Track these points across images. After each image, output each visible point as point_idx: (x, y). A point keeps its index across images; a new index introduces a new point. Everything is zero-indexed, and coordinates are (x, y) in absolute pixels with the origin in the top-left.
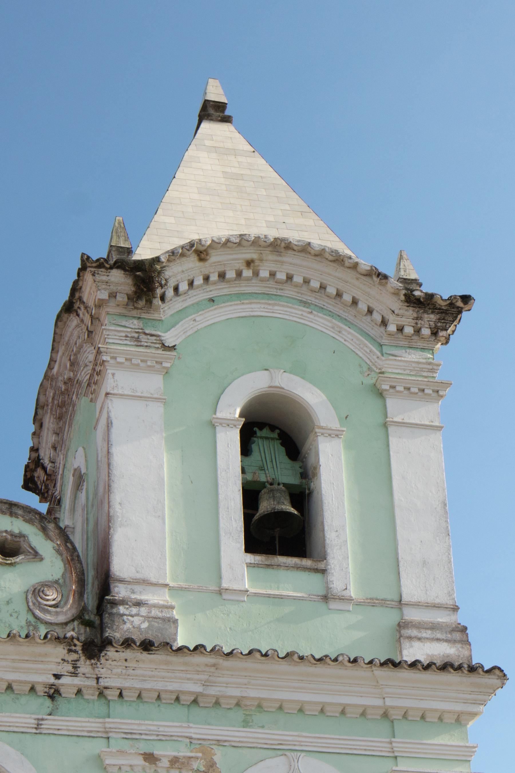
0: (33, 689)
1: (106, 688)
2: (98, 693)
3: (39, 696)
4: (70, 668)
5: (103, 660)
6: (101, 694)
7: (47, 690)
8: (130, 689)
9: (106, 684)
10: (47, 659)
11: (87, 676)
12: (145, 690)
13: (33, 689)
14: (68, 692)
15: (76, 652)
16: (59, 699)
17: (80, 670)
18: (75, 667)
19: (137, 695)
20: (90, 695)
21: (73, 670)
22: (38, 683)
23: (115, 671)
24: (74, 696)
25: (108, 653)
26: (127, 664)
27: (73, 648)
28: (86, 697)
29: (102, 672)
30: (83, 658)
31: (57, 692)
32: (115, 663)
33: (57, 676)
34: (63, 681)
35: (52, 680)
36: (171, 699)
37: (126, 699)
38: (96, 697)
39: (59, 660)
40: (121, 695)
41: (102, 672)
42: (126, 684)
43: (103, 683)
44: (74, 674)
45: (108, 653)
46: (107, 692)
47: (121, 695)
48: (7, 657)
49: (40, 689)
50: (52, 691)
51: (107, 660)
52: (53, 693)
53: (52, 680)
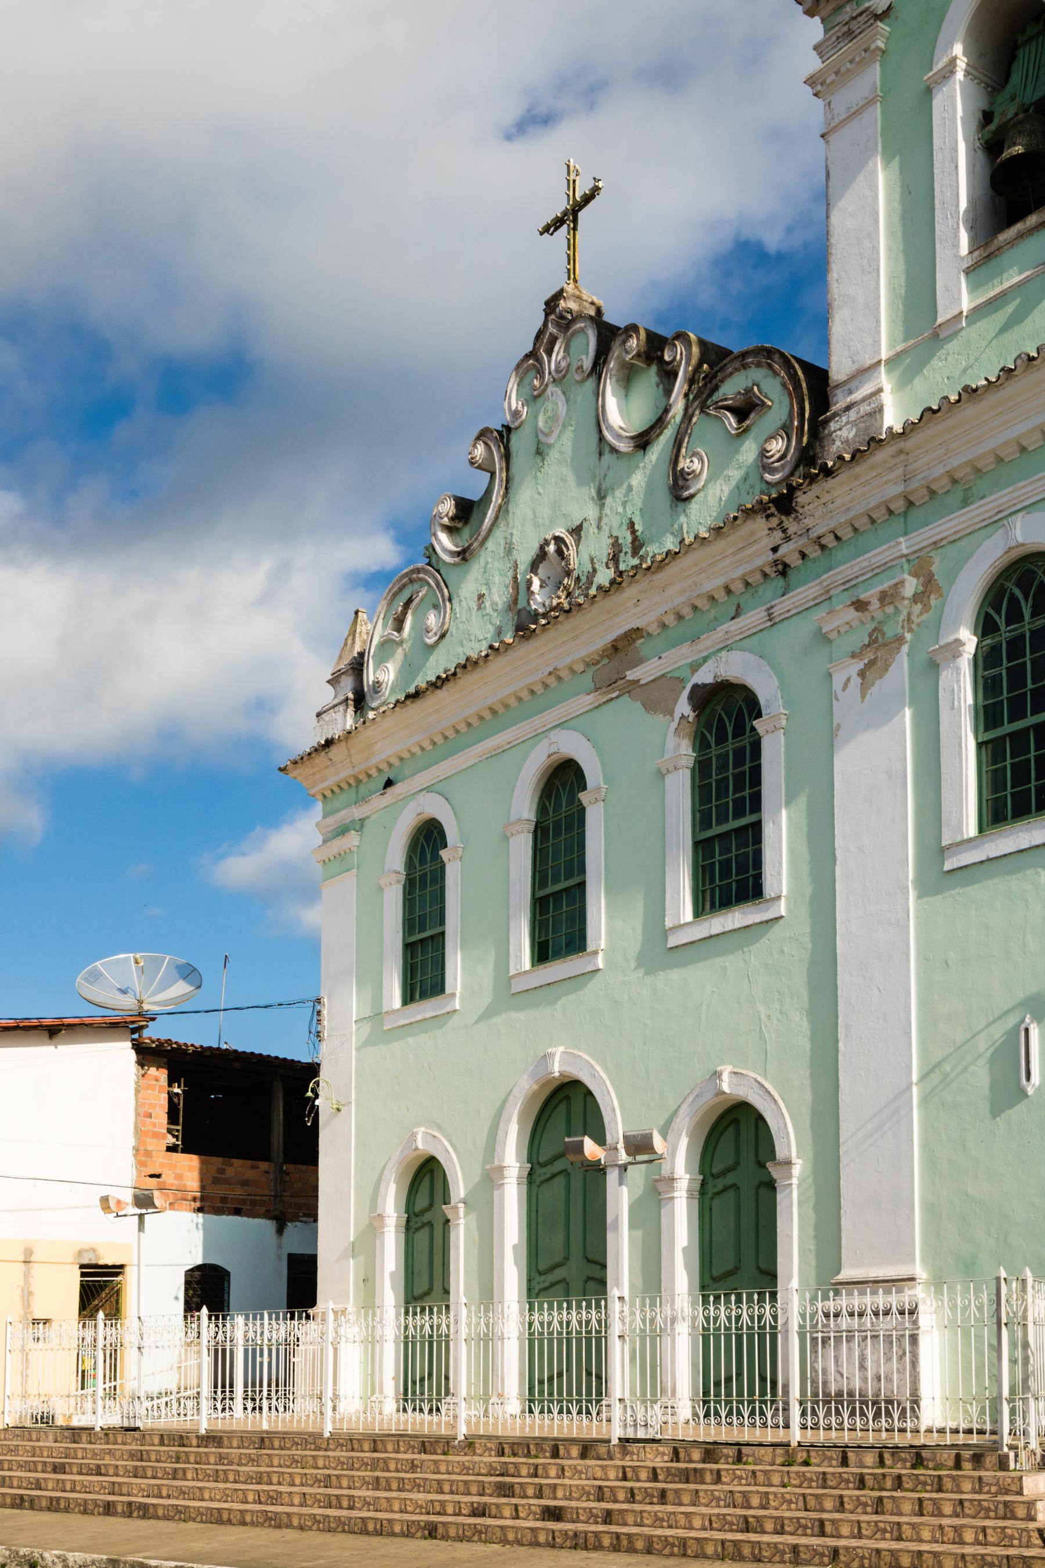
0: (765, 575)
1: (819, 538)
2: (817, 547)
3: (773, 579)
4: (778, 534)
5: (801, 510)
6: (823, 547)
7: (774, 569)
8: (840, 525)
9: (815, 534)
10: (758, 536)
11: (799, 533)
12: (853, 518)
13: (765, 575)
14: (794, 560)
15: (772, 515)
16: (791, 573)
17: (790, 532)
18: (784, 531)
19: (850, 528)
20: (814, 553)
21: (783, 535)
22: (764, 565)
23: (817, 515)
24: (801, 562)
25: (799, 500)
26: (823, 501)
27: (769, 512)
28: (812, 556)
29: (808, 522)
30: (783, 518)
31: (786, 566)
32: (811, 506)
33: (775, 550)
34: (782, 551)
35: (771, 556)
36: (884, 515)
37: (844, 539)
38: (819, 552)
39: (767, 532)
40: (837, 538)
41: (808, 522)
42: (833, 524)
43: (814, 534)
44: (788, 539)
45: (799, 500)
46: (823, 541)
47: (837, 538)
48: (726, 554)
49: (768, 570)
50: (780, 567)
51: (803, 507)
52: (784, 569)
53: (771, 556)
